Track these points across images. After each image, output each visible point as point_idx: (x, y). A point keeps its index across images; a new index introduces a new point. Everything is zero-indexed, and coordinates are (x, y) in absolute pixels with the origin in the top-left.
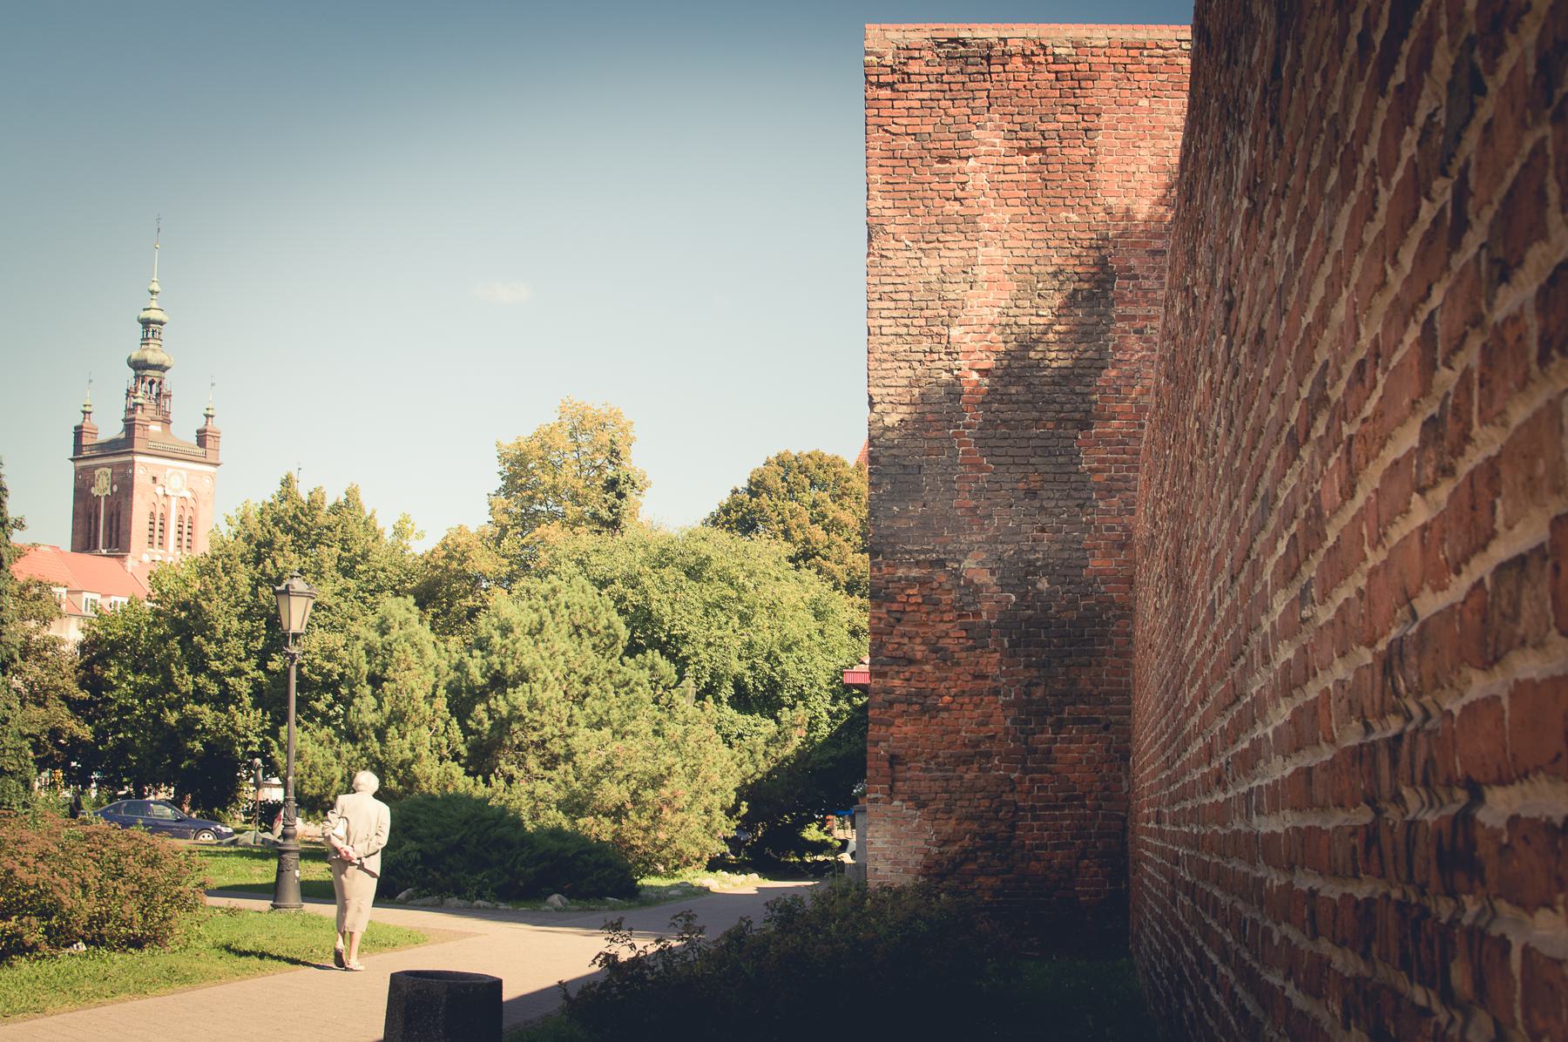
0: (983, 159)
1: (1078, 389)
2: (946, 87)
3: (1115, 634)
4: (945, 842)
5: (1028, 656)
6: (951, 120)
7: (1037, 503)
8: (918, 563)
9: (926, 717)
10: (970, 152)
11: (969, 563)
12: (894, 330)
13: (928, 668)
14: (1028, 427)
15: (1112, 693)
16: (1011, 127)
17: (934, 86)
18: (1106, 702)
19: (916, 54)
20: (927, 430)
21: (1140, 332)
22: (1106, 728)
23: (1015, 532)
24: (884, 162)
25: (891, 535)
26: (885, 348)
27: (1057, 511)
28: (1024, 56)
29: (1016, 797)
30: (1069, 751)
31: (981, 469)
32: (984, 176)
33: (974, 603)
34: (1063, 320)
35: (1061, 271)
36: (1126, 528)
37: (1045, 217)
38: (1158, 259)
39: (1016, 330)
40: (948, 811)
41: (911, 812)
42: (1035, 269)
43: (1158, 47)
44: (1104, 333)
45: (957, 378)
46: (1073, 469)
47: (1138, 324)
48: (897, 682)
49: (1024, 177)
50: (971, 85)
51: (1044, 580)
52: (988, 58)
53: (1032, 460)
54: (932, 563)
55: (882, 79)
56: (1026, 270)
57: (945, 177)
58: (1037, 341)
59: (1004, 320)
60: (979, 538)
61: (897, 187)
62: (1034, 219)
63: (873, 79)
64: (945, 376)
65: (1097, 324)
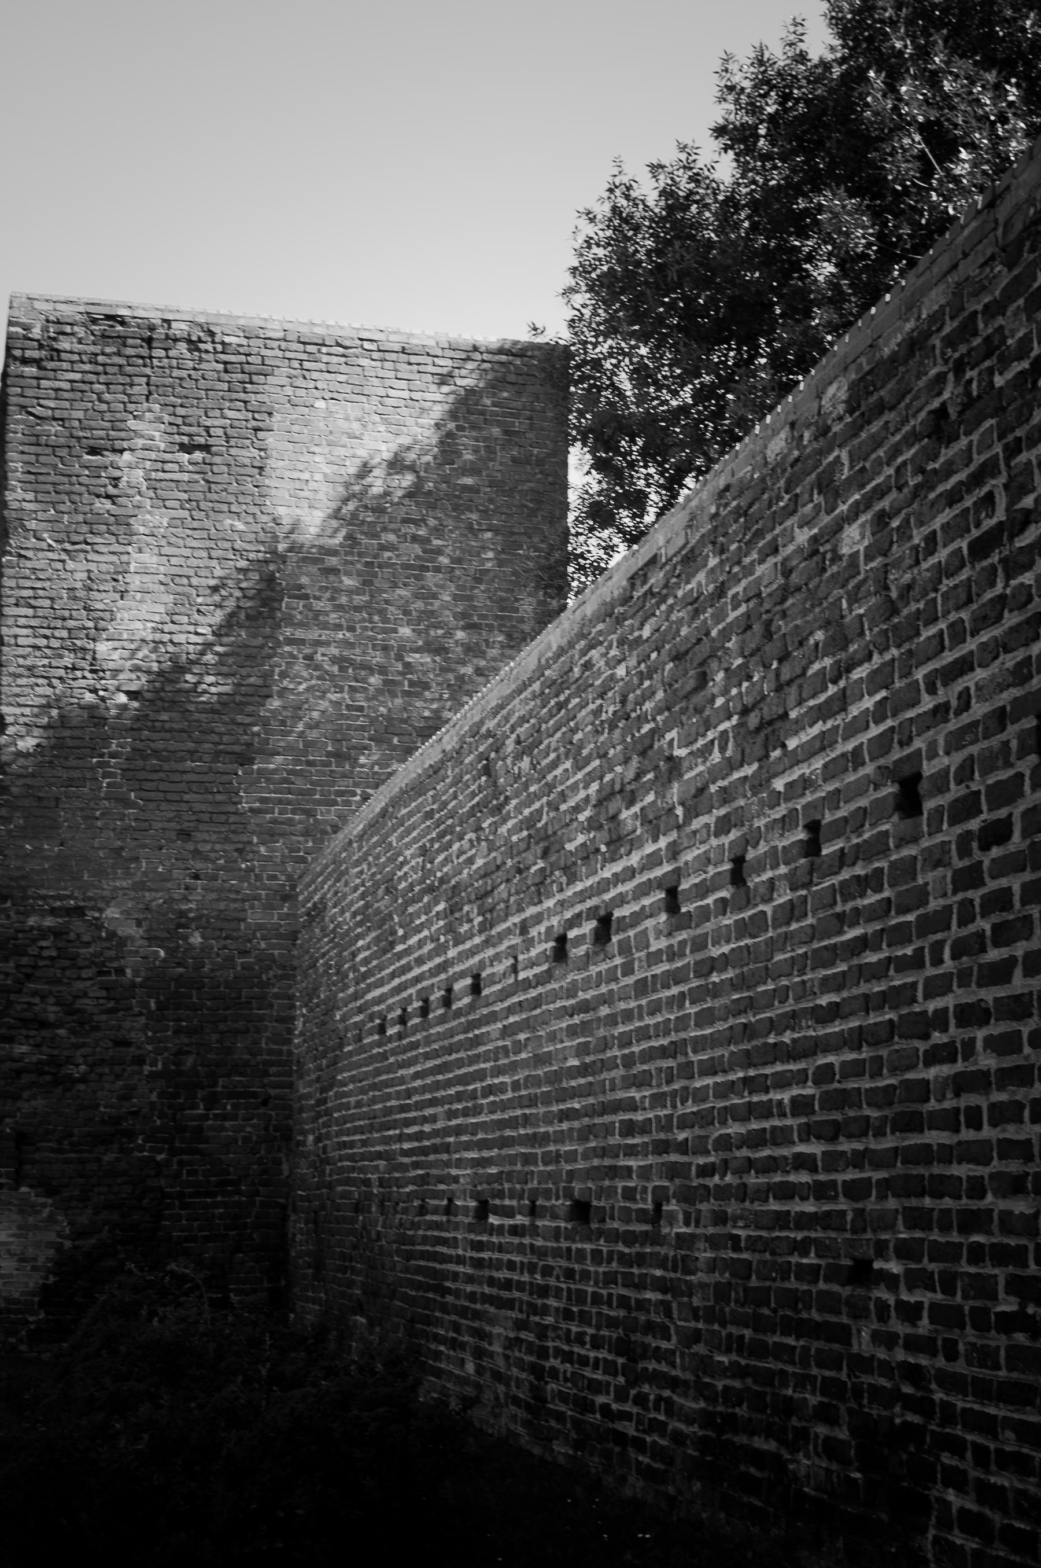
0: (141, 454)
1: (239, 718)
2: (100, 368)
3: (276, 996)
5: (178, 1020)
6: (104, 407)
7: (190, 846)
8: (53, 911)
9: (59, 1090)
10: (125, 444)
11: (112, 913)
12: (31, 641)
13: (62, 1032)
14: (182, 760)
15: (272, 1064)
16: (172, 419)
17: (87, 367)
18: (266, 1074)
19: (68, 329)
20: (66, 758)
21: (309, 658)
22: (265, 1103)
23: (165, 878)
24: (26, 448)
25: (23, 877)
26: (21, 661)
27: (213, 855)
28: (189, 341)
29: (163, 1182)
30: (224, 1129)
31: (128, 804)
32: (140, 473)
33: (117, 958)
34: (225, 640)
35: (224, 586)
36: (290, 878)
37: (208, 524)
38: (332, 578)
39: (171, 648)
41: (41, 1200)
42: (195, 581)
43: (338, 345)
44: (270, 657)
45: (103, 699)
46: (231, 808)
47: (308, 651)
48: (24, 1049)
49: (185, 477)
50: (128, 369)
51: (197, 934)
52: (149, 341)
53: (186, 797)
54: (69, 912)
55: (28, 354)
56: (185, 581)
57: (96, 471)
58: (192, 662)
59: (158, 636)
60: (124, 884)
61: (41, 478)
62: (195, 524)
63: (18, 353)
64: (89, 697)
65: (262, 647)
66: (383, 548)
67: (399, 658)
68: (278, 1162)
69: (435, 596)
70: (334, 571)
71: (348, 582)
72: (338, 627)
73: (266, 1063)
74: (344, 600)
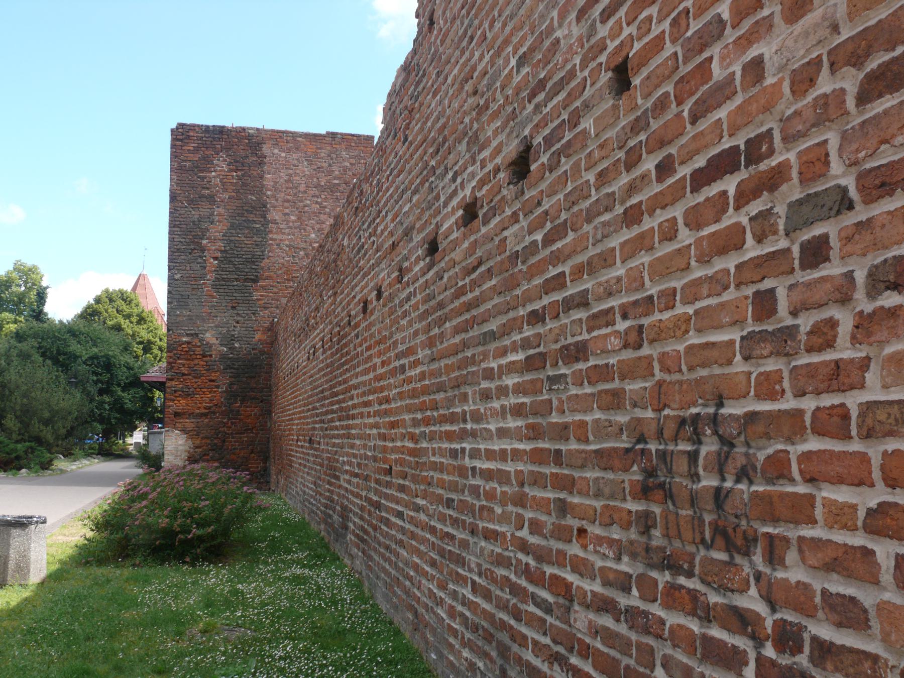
4: (197, 447)
7: (236, 312)
11: (208, 335)
21: (278, 245)
31: (213, 297)
40: (197, 435)
47: (278, 242)
66: (305, 206)
67: (311, 245)
68: (266, 422)
69: (323, 223)
70: (288, 214)
71: (293, 218)
72: (289, 234)
73: (263, 388)
74: (291, 224)
